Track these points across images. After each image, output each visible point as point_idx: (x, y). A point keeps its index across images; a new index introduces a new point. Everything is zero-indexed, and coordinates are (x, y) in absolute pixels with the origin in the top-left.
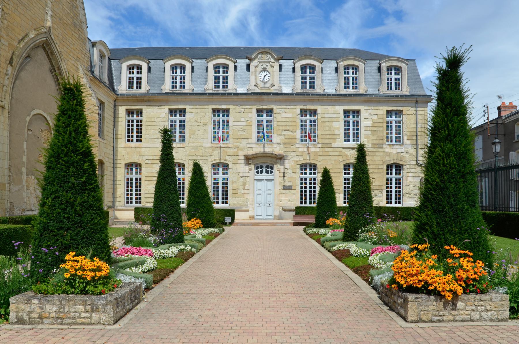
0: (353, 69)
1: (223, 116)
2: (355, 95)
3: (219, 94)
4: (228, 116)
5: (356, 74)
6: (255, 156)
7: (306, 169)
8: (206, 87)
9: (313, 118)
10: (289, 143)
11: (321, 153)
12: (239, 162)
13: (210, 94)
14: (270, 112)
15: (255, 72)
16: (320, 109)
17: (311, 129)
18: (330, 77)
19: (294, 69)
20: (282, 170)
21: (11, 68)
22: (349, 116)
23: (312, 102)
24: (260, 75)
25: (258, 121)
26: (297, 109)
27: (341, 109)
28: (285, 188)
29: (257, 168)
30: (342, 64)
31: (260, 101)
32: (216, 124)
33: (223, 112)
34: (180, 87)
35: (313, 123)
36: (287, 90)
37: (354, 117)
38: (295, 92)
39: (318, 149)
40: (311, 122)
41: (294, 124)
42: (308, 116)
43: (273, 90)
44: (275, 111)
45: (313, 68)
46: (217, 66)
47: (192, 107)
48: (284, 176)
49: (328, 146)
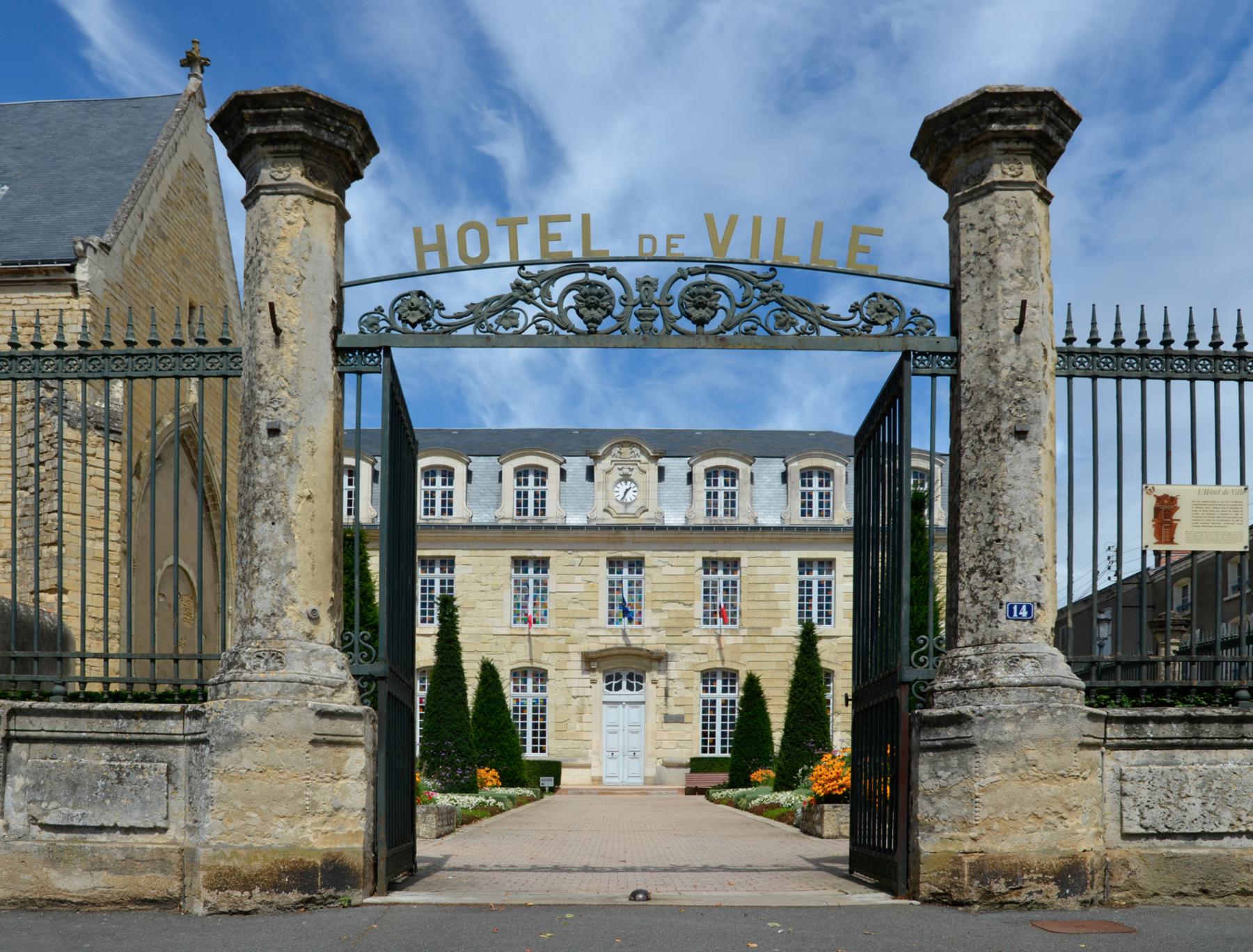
0: (820, 475)
1: (535, 572)
2: (825, 529)
3: (527, 527)
4: (546, 572)
5: (828, 485)
6: (604, 654)
7: (713, 682)
8: (498, 513)
9: (730, 577)
10: (678, 628)
11: (747, 648)
12: (569, 665)
13: (506, 527)
14: (637, 564)
15: (606, 482)
16: (745, 557)
17: (725, 599)
18: (769, 492)
19: (690, 476)
20: (662, 683)
21: (138, 481)
22: (809, 572)
23: (729, 544)
24: (616, 489)
25: (611, 583)
26: (697, 558)
27: (792, 557)
28: (668, 719)
29: (608, 679)
30: (796, 466)
31: (615, 542)
32: (521, 587)
33: (535, 565)
34: (443, 512)
35: (730, 588)
36: (674, 518)
37: (821, 572)
38: (691, 523)
39: (740, 640)
40: (725, 583)
41: (689, 588)
42: (720, 573)
43: (644, 519)
44: (647, 563)
45: (732, 474)
46: (522, 470)
47: (467, 553)
48: (667, 696)
49: (764, 632)
